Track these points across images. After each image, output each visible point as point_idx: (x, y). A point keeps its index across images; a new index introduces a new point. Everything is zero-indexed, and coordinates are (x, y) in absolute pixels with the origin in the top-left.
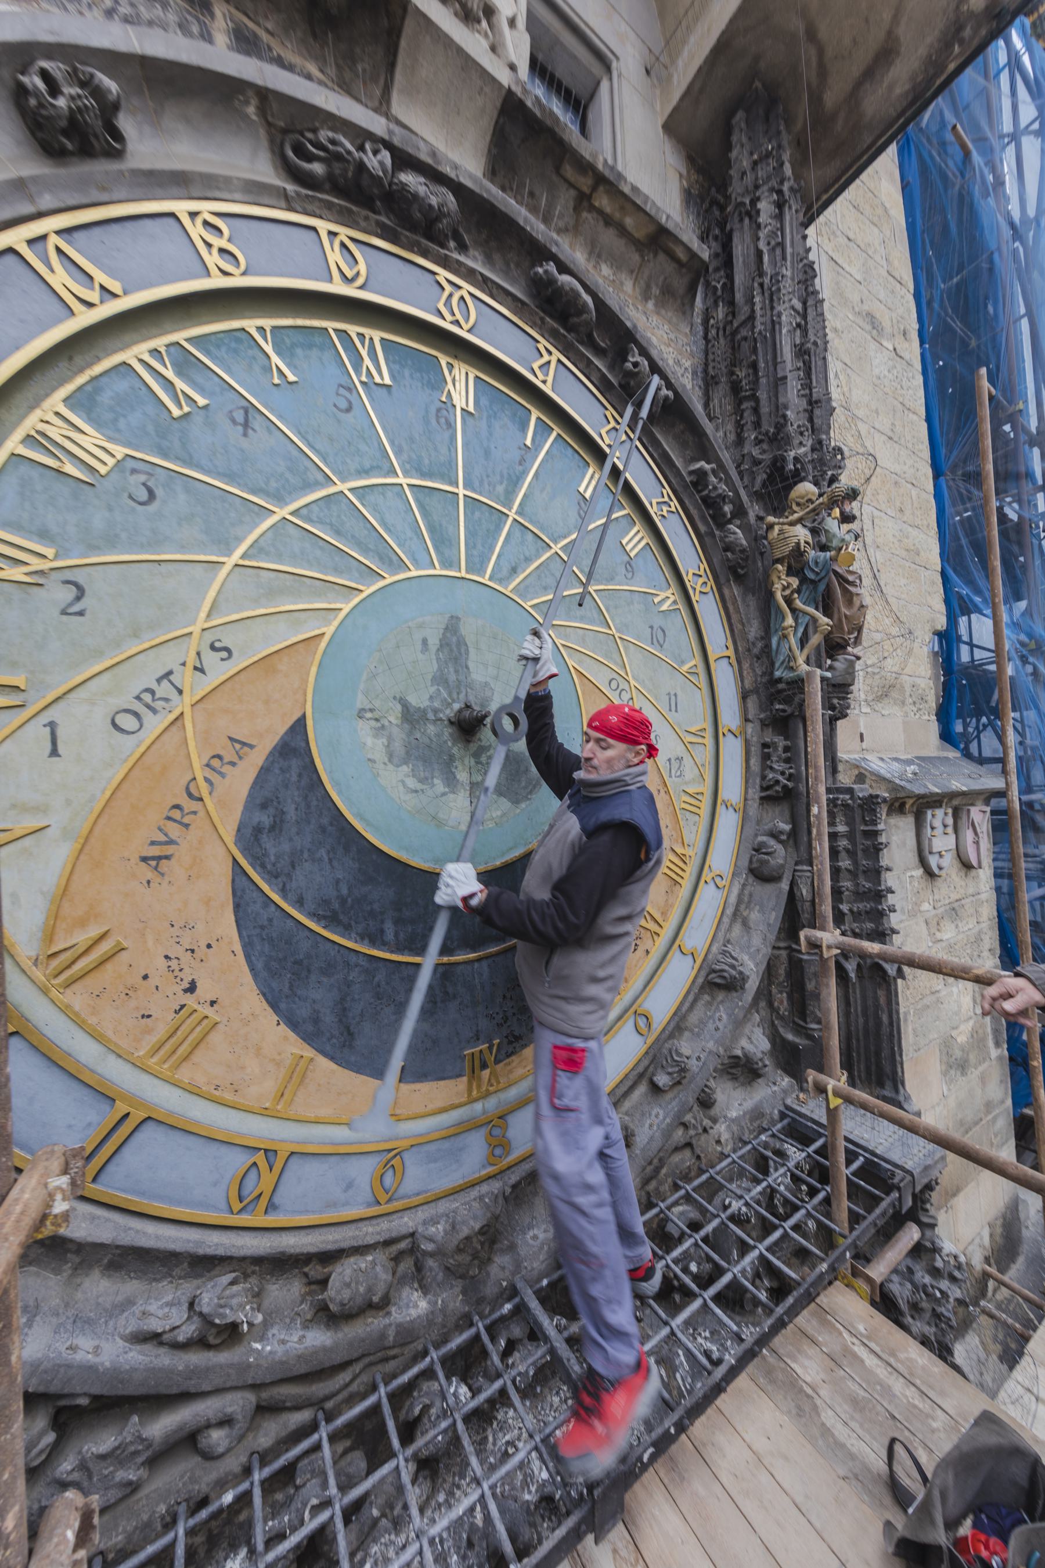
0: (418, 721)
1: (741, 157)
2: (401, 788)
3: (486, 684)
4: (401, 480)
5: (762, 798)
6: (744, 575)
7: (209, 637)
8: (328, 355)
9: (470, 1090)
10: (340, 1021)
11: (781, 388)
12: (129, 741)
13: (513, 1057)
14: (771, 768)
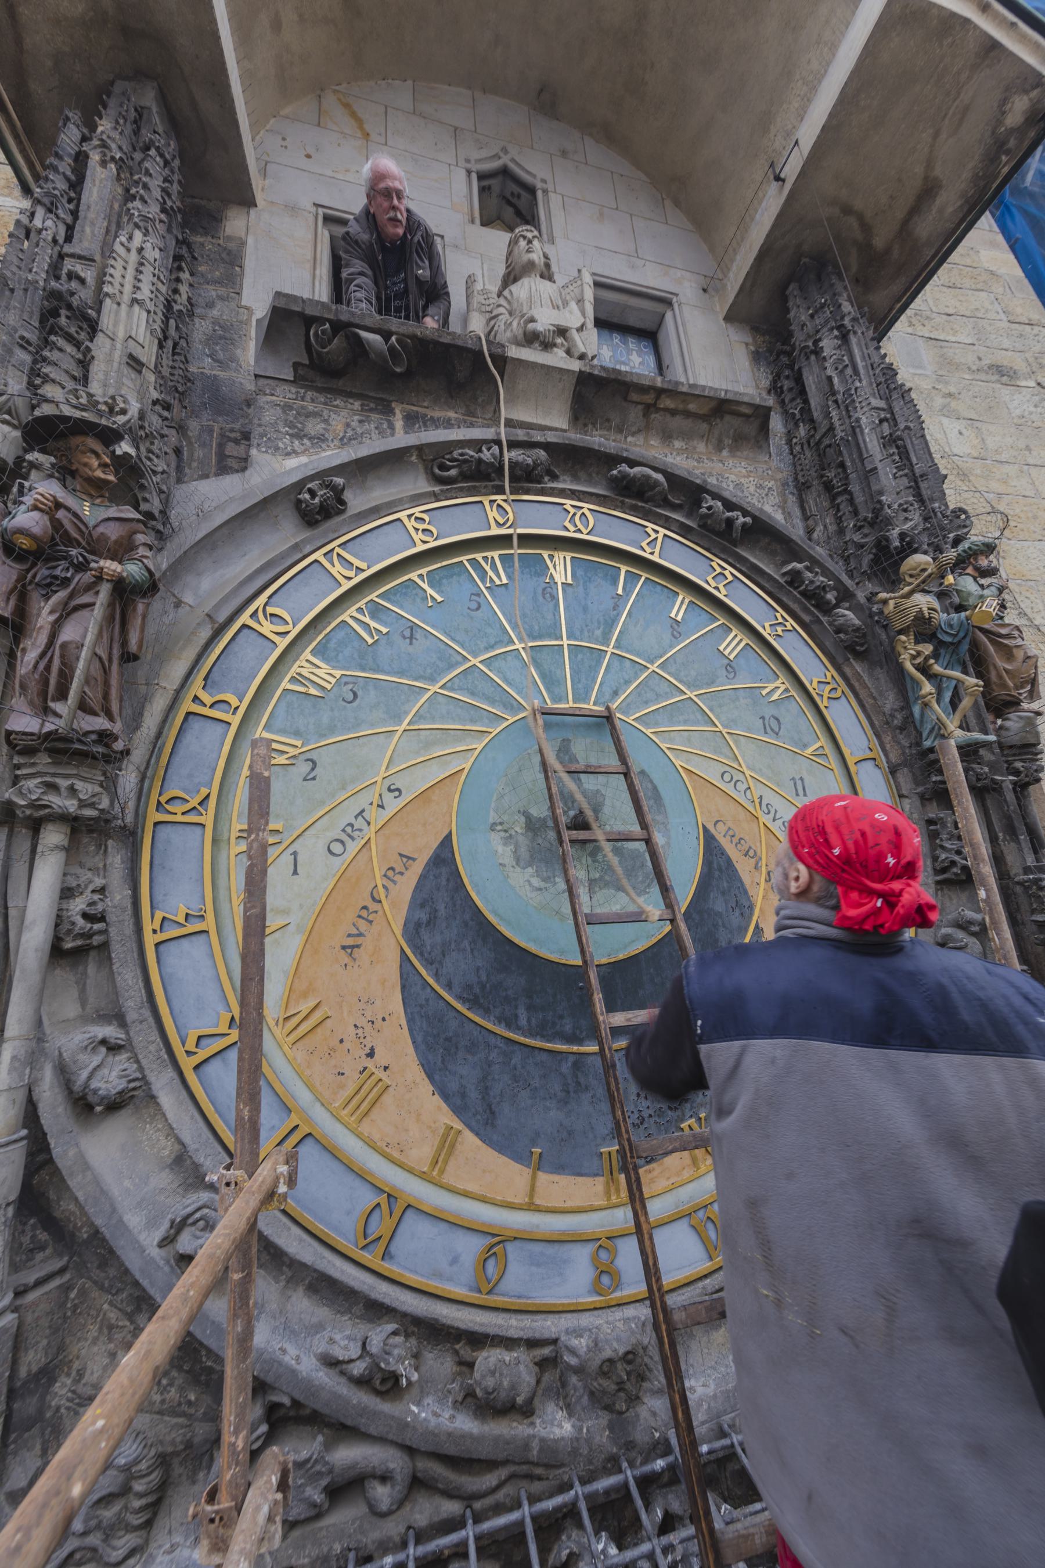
1: (799, 314)
2: (528, 887)
3: (598, 791)
4: (519, 646)
5: (938, 883)
7: (387, 783)
8: (464, 577)
9: (608, 1194)
11: (872, 479)
12: (337, 861)
13: (653, 1165)
14: (942, 847)
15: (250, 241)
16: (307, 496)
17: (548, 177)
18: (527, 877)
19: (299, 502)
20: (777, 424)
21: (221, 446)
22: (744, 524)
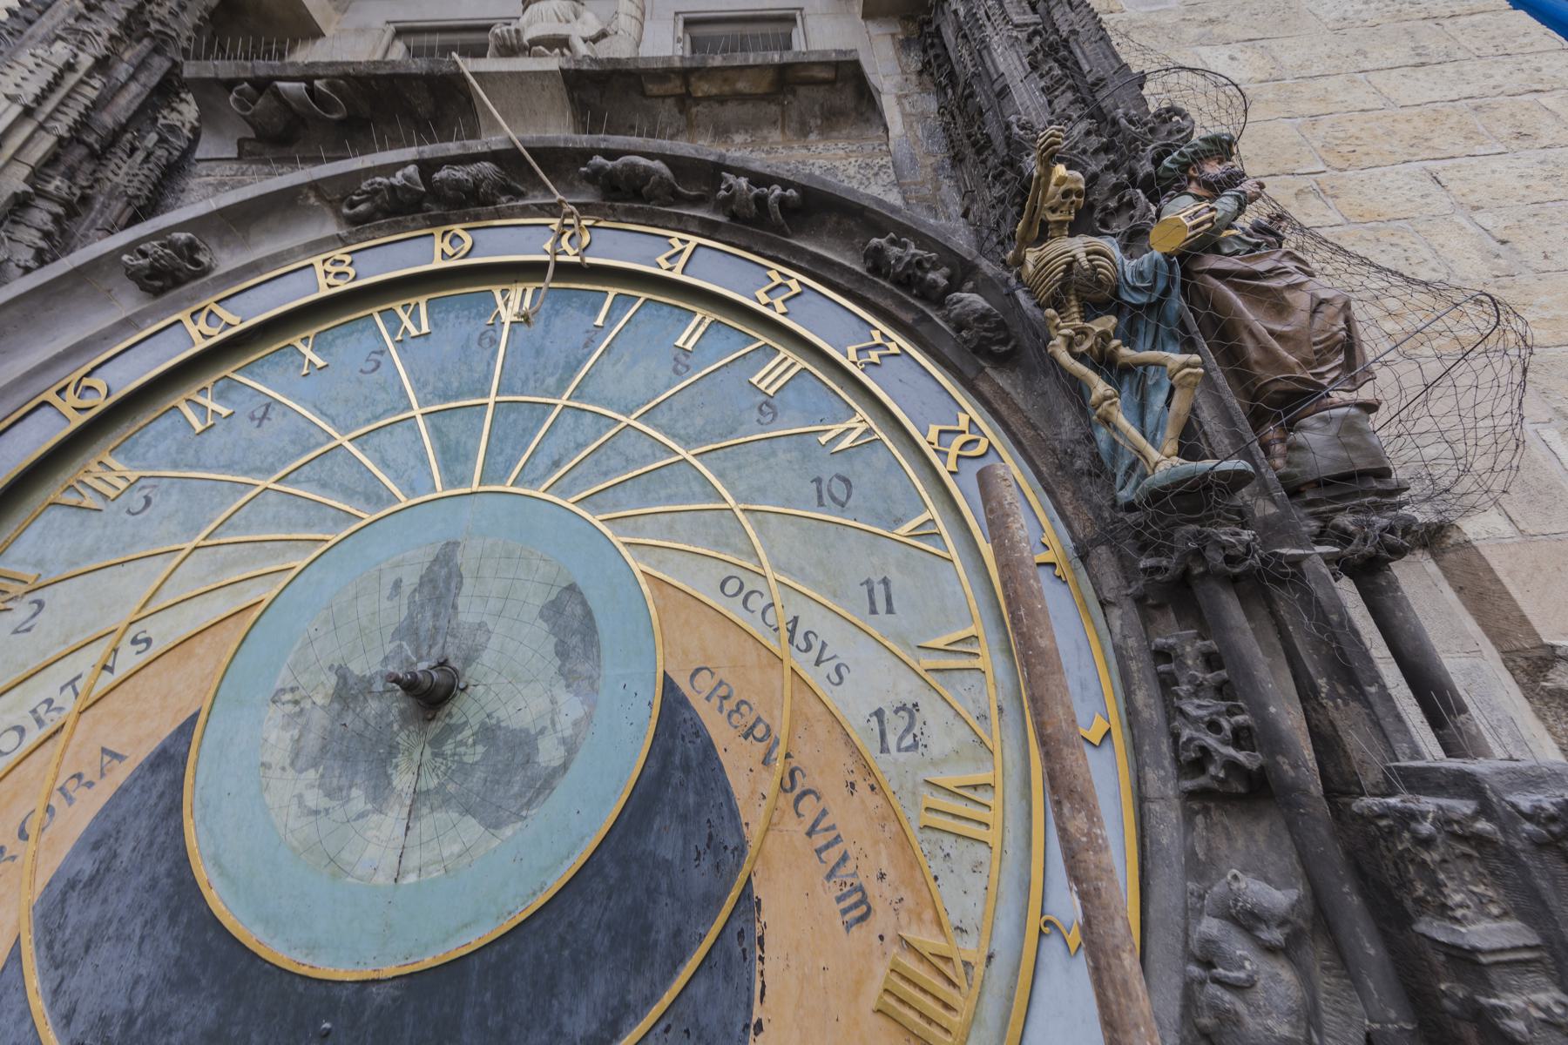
0: (355, 697)
3: (481, 625)
22: (782, 201)
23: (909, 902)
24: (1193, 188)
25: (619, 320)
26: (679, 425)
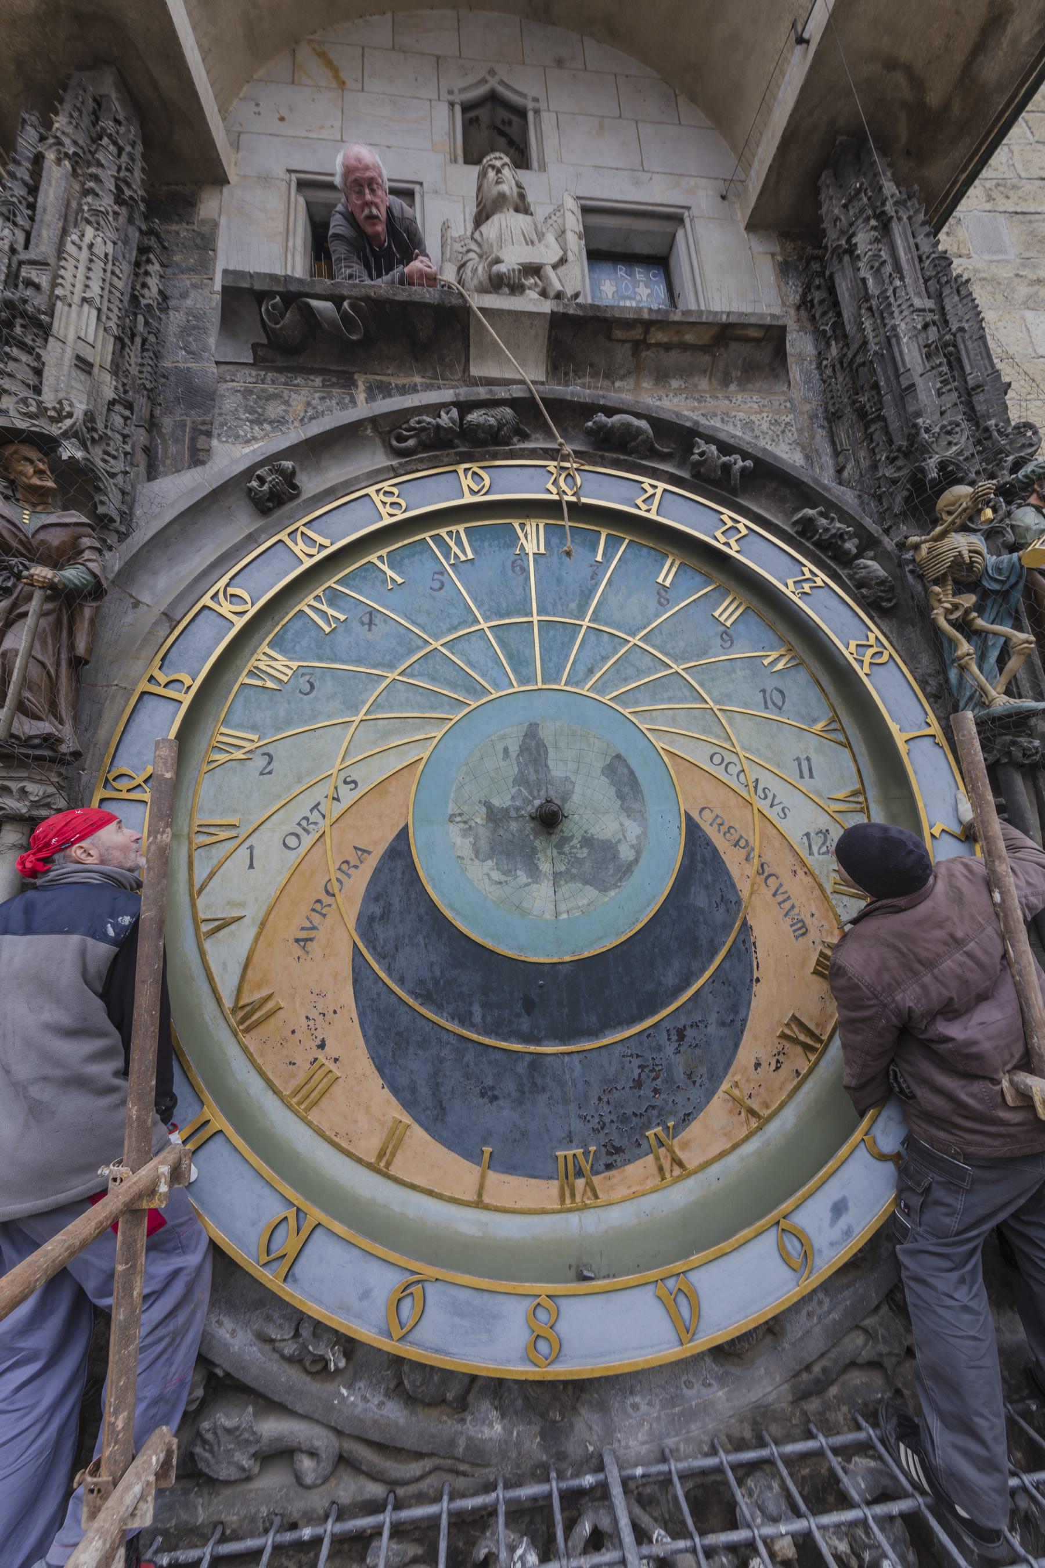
0: (501, 820)
1: (832, 206)
2: (487, 881)
3: (567, 778)
4: (484, 625)
6: (892, 608)
7: (343, 775)
10: (434, 1094)
11: (908, 399)
13: (614, 1172)
15: (223, 221)
16: (254, 484)
17: (541, 96)
18: (486, 870)
19: (250, 490)
20: (800, 345)
21: (193, 440)
22: (744, 469)
23: (826, 926)
24: (1033, 499)
25: (613, 557)
26: (669, 646)
